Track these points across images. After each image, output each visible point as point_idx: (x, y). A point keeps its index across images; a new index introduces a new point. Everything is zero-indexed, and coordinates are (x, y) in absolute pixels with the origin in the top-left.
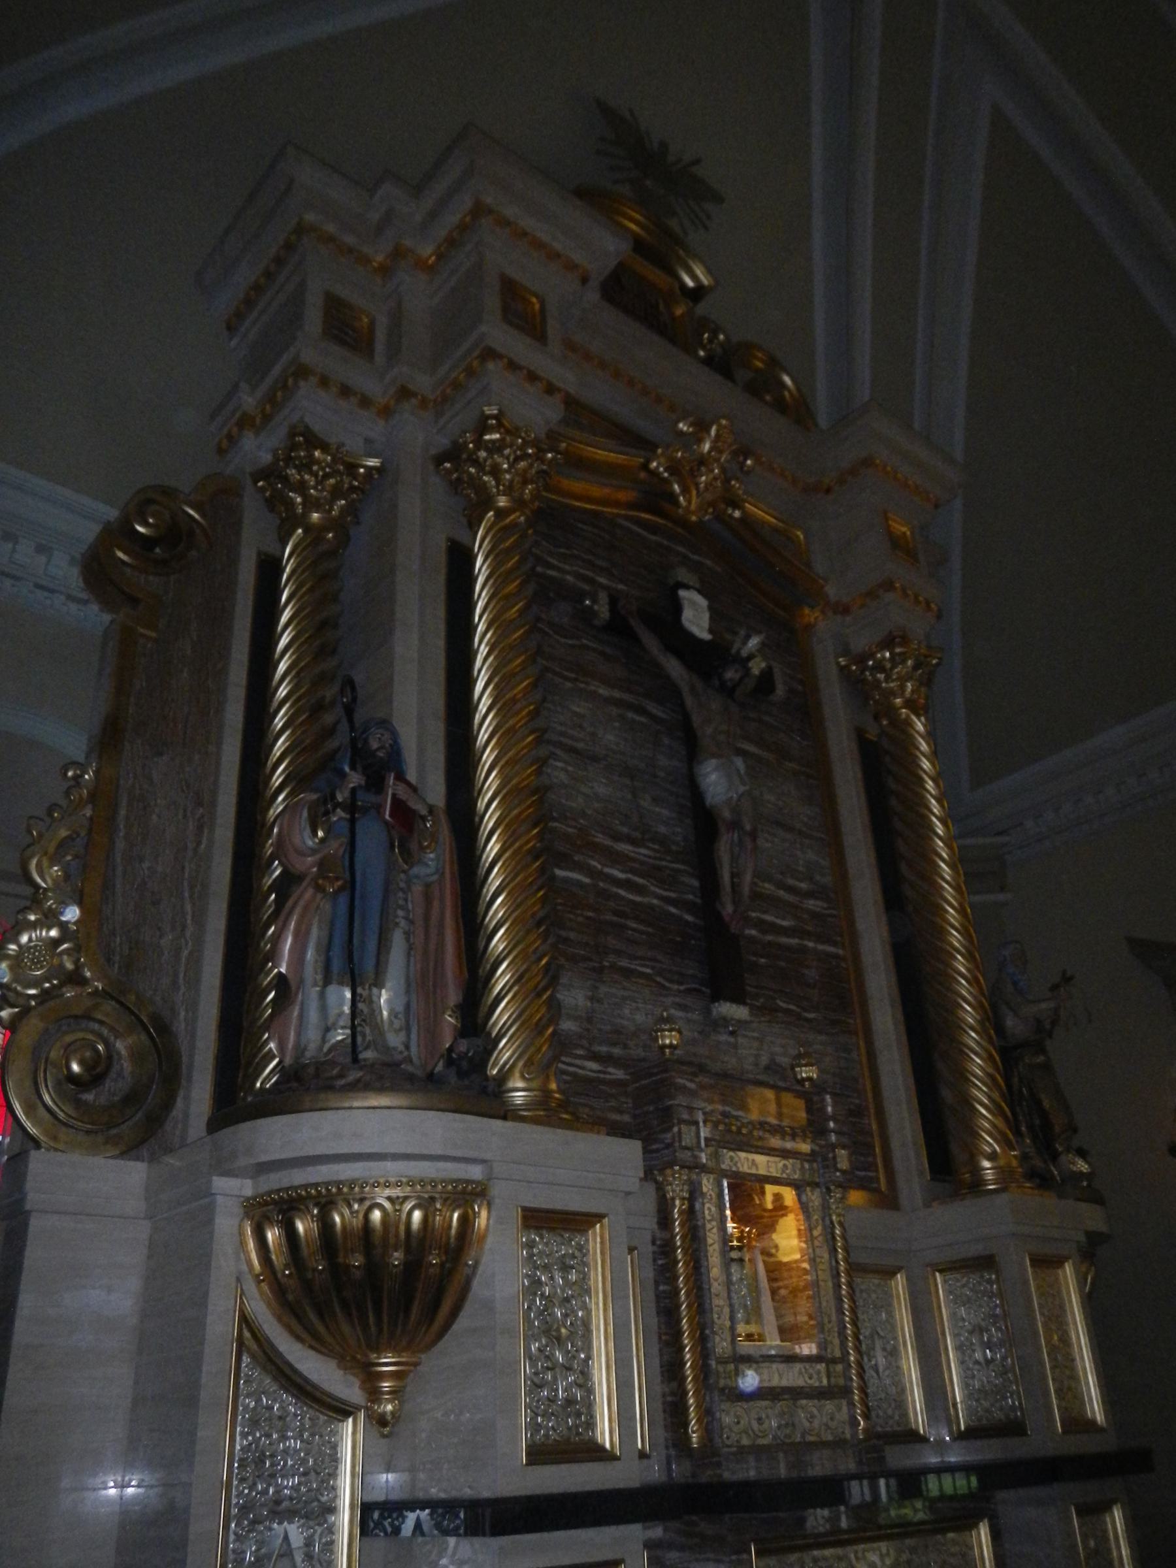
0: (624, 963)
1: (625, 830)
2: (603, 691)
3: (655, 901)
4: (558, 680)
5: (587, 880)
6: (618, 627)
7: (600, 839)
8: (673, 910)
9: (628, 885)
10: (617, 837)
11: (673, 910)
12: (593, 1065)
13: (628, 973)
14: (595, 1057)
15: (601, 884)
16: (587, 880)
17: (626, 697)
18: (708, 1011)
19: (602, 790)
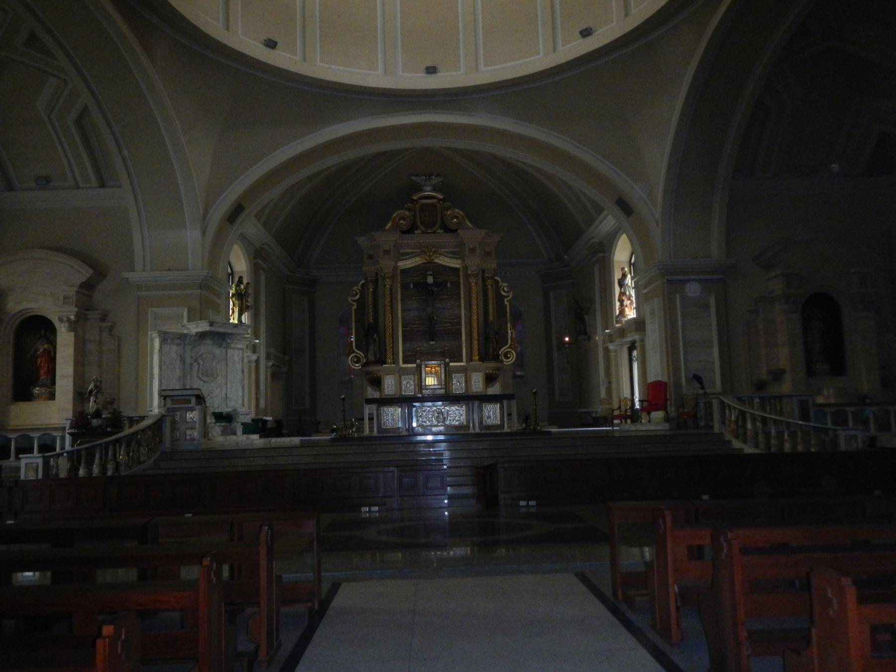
2: (414, 298)
9: (417, 328)
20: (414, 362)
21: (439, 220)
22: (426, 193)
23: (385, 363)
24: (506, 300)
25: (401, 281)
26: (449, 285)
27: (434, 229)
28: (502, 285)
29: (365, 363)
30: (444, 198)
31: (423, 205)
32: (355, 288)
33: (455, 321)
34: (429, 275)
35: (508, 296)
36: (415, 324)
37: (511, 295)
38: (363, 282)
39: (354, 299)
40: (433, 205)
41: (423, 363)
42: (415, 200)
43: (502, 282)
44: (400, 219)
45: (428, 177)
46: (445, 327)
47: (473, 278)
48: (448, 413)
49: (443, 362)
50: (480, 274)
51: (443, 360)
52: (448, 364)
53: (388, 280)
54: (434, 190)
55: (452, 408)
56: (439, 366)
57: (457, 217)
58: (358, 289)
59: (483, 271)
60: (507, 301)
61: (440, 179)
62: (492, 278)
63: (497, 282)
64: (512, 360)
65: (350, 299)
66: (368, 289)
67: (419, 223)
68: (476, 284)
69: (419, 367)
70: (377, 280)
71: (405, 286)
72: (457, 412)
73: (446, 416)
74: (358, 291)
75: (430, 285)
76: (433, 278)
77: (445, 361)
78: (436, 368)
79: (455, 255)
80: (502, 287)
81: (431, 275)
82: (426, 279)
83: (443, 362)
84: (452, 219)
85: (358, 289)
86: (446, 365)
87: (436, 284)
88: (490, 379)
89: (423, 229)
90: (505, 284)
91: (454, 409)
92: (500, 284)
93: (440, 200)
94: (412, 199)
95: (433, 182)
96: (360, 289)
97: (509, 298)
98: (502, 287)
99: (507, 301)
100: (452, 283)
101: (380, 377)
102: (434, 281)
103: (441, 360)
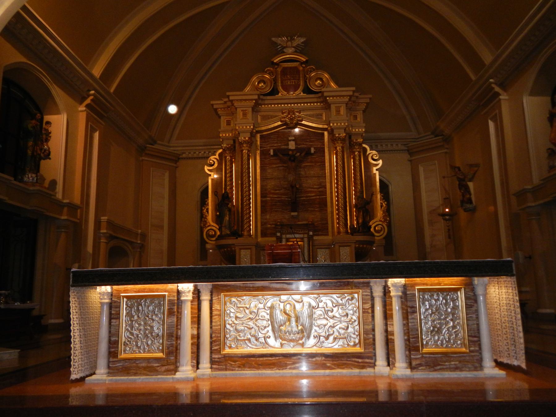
0: (276, 210)
1: (277, 189)
2: (274, 166)
3: (283, 199)
4: (265, 168)
5: (269, 199)
6: (275, 154)
7: (273, 191)
8: (287, 199)
10: (276, 190)
11: (287, 199)
12: (270, 226)
13: (276, 211)
14: (270, 224)
15: (272, 199)
16: (269, 199)
17: (279, 165)
18: (291, 214)
19: (273, 183)
21: (302, 83)
22: (288, 56)
23: (241, 236)
24: (375, 169)
25: (261, 147)
26: (313, 150)
28: (370, 154)
29: (219, 236)
30: (306, 62)
31: (285, 69)
32: (212, 158)
33: (320, 190)
34: (290, 140)
35: (377, 165)
37: (380, 162)
38: (221, 151)
39: (211, 168)
41: (284, 236)
42: (277, 64)
43: (371, 150)
44: (258, 83)
45: (289, 38)
46: (307, 197)
47: (339, 142)
48: (311, 316)
49: (306, 236)
50: (347, 138)
51: (306, 233)
52: (312, 236)
53: (245, 145)
54: (295, 52)
55: (324, 299)
56: (302, 240)
57: (321, 79)
58: (215, 158)
59: (350, 137)
60: (377, 170)
61: (303, 40)
62: (360, 145)
63: (365, 150)
64: (381, 235)
65: (206, 168)
66: (226, 157)
67: (280, 87)
68: (343, 147)
71: (264, 154)
72: (337, 312)
73: (307, 322)
74: (215, 160)
76: (296, 144)
77: (308, 234)
78: (299, 243)
79: (317, 118)
80: (371, 155)
81: (293, 140)
82: (288, 145)
83: (306, 236)
84: (316, 81)
85: (215, 158)
86: (310, 238)
87: (297, 150)
88: (360, 254)
90: (374, 152)
91: (330, 304)
92: (369, 151)
93: (302, 63)
94: (273, 63)
95: (295, 44)
96: (218, 158)
97: (378, 167)
98: (371, 155)
99: (377, 170)
100: (315, 148)
101: (235, 251)
102: (295, 147)
103: (304, 234)
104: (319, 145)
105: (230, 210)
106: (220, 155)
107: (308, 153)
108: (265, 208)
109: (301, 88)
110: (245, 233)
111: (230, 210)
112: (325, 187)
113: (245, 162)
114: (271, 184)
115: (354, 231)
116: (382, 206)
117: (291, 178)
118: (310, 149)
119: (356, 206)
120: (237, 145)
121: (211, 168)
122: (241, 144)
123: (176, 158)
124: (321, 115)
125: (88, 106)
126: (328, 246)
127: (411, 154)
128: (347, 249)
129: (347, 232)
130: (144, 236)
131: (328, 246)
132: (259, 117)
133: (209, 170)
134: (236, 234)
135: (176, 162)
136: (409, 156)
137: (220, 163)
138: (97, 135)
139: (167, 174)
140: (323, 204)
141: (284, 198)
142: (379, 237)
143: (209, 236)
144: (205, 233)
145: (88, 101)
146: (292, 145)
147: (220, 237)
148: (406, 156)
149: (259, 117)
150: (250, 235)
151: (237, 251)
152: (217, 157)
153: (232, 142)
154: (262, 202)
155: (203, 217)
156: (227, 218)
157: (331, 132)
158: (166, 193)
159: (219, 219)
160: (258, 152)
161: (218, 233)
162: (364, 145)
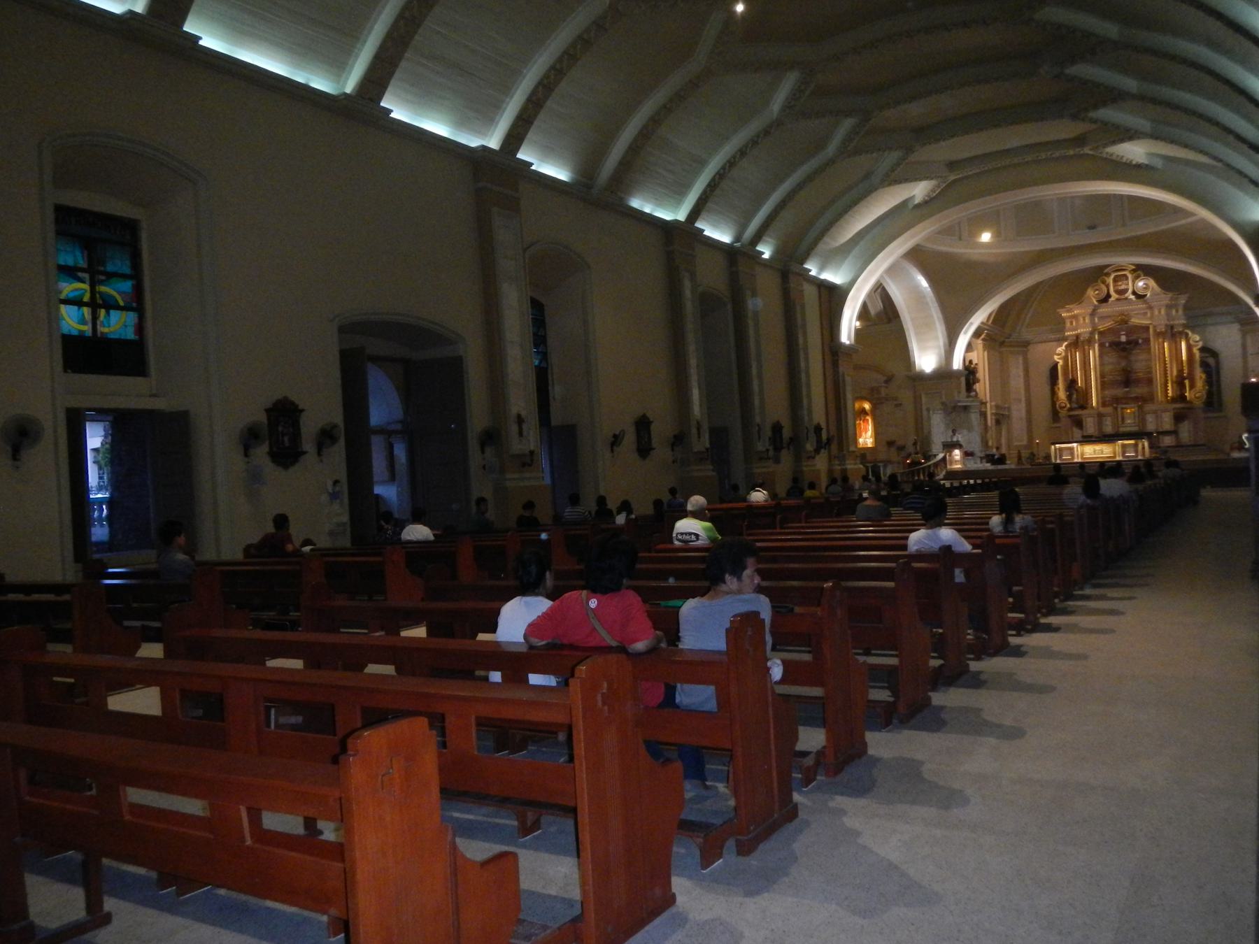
6: (1110, 346)
20: (1112, 405)
26: (1140, 341)
27: (1126, 295)
31: (1116, 276)
36: (1111, 375)
40: (1125, 275)
63: (1187, 335)
69: (1116, 409)
70: (1077, 342)
71: (1101, 345)
75: (1124, 343)
81: (1124, 334)
82: (1119, 338)
86: (1140, 408)
87: (1128, 342)
88: (1179, 418)
89: (1117, 296)
97: (1199, 347)
100: (1143, 339)
104: (1144, 336)
105: (1076, 390)
106: (1066, 347)
107: (1137, 343)
108: (1103, 385)
109: (1130, 291)
110: (1089, 405)
111: (1076, 390)
112: (1151, 368)
113: (1087, 352)
114: (1108, 368)
115: (1174, 400)
116: (1201, 378)
117: (1123, 364)
118: (1138, 341)
119: (1176, 382)
120: (1080, 343)
121: (1059, 357)
122: (1083, 342)
123: (1026, 344)
124: (1146, 313)
125: (983, 340)
126: (1155, 412)
127: (1242, 325)
128: (1168, 414)
129: (1168, 401)
130: (1009, 409)
131: (1155, 412)
132: (1096, 319)
133: (1059, 359)
134: (1083, 407)
135: (1026, 347)
136: (1239, 327)
137: (1066, 351)
138: (986, 353)
139: (1021, 359)
140: (1150, 381)
141: (1119, 378)
142: (1198, 403)
143: (1062, 408)
144: (1057, 406)
145: (983, 336)
146: (1123, 339)
147: (1071, 409)
148: (1235, 328)
149: (1096, 319)
150: (1092, 407)
151: (1084, 419)
152: (1063, 347)
153: (1075, 338)
154: (1101, 381)
155: (1053, 393)
156: (1075, 396)
157: (1155, 327)
158: (1021, 374)
159: (1069, 397)
160: (1097, 345)
161: (1068, 406)
162: (1187, 331)
